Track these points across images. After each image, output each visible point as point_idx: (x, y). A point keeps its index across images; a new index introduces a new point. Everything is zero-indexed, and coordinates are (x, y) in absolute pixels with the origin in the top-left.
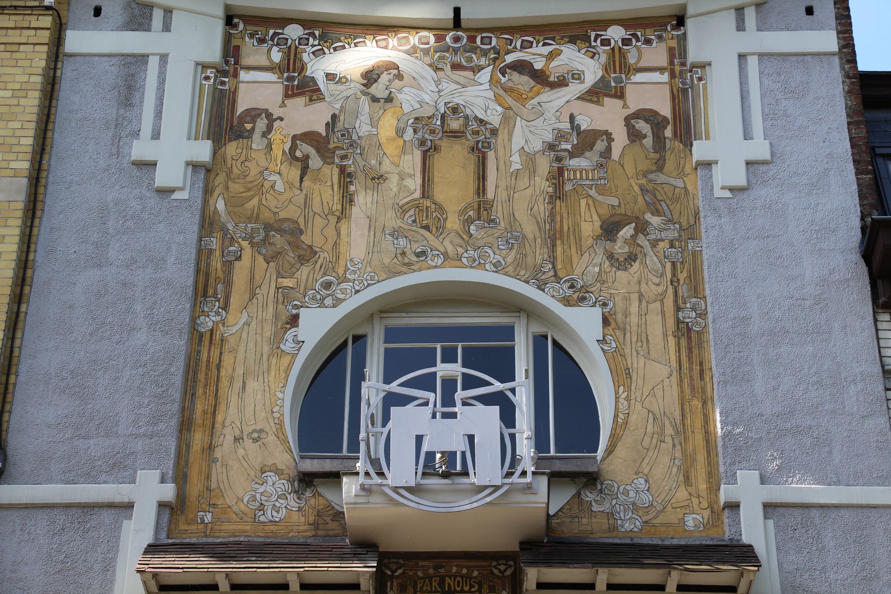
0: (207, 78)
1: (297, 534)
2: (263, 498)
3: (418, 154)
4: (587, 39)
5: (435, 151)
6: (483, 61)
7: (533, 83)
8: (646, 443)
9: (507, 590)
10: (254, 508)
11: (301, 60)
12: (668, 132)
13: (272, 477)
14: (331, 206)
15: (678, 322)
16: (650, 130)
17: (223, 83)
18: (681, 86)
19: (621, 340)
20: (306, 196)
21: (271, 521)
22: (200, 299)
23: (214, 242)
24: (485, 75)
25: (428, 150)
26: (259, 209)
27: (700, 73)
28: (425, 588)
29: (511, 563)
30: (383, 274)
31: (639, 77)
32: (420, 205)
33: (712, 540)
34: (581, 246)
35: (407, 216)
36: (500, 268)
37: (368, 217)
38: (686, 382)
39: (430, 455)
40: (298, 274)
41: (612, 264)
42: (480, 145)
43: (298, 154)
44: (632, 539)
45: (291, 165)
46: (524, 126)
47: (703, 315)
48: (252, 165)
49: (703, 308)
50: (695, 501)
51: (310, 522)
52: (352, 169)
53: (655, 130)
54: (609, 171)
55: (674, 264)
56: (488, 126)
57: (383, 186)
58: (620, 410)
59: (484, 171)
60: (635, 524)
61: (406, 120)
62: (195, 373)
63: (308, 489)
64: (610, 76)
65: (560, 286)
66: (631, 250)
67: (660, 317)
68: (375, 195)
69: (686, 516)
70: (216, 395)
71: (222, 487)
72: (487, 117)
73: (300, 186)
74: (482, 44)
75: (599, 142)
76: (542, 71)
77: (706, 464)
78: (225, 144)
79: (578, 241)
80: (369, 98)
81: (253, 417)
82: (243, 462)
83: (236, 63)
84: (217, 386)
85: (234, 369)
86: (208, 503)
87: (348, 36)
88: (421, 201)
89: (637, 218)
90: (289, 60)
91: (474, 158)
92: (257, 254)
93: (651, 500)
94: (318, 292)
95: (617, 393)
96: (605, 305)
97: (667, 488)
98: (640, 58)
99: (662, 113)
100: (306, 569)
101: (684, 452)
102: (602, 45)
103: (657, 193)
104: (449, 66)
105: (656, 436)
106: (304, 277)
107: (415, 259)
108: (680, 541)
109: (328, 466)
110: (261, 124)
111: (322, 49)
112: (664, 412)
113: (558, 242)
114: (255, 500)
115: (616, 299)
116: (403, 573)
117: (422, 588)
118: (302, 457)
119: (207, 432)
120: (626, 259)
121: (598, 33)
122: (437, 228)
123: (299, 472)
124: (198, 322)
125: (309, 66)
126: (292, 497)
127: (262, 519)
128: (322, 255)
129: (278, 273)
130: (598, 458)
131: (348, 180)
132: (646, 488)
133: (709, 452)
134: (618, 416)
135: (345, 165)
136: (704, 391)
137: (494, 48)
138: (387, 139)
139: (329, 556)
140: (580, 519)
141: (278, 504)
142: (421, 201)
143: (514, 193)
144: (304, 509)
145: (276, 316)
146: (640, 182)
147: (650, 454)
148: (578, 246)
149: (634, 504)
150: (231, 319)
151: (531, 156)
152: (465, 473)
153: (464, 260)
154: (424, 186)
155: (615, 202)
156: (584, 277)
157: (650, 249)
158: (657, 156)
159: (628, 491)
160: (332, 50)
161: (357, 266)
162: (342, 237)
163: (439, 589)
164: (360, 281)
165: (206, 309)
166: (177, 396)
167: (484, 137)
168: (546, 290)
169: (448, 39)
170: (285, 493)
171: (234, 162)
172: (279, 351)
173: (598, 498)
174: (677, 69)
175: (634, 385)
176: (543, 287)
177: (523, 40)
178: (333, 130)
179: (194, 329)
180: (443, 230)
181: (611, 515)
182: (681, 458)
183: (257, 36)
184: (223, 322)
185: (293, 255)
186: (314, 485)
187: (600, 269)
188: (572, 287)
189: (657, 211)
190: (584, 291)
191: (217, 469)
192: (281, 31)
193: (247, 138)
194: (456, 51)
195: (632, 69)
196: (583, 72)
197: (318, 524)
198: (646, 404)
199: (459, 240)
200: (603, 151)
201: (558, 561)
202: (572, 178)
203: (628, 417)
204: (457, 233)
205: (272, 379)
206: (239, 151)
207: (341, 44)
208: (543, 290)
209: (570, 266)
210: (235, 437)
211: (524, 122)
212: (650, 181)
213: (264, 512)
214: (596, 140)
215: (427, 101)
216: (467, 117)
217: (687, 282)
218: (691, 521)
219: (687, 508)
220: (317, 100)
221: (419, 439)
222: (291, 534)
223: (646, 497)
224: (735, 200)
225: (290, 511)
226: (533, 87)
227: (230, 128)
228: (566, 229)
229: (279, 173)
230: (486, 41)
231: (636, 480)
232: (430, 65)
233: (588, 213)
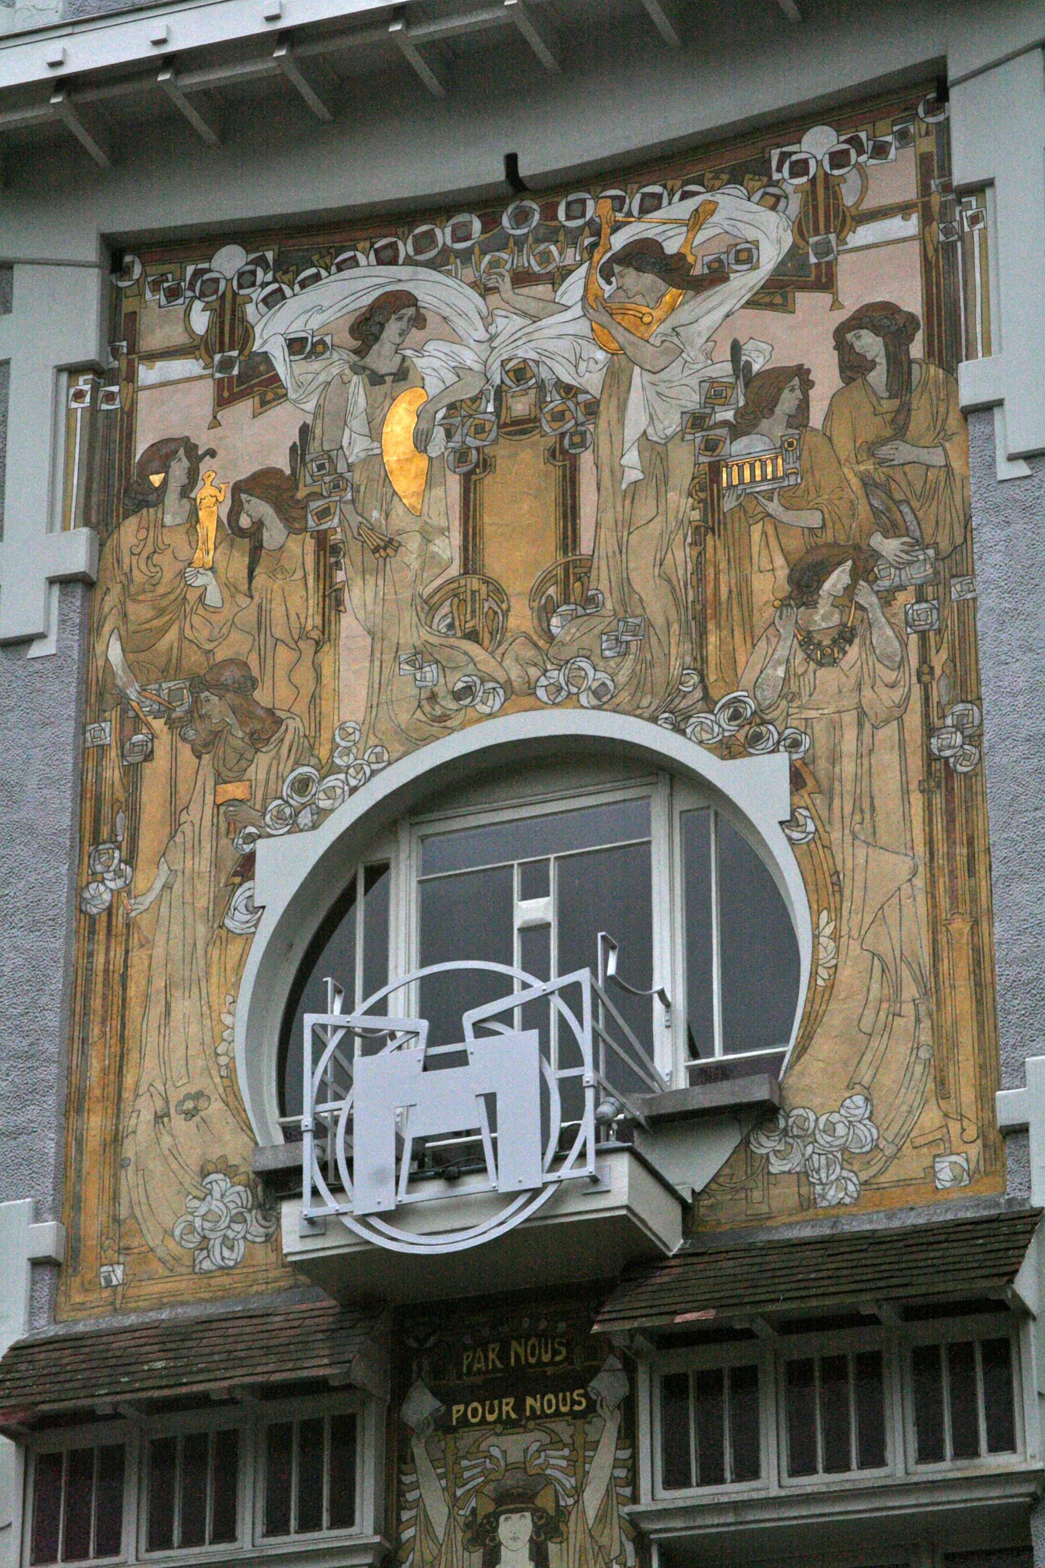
0: (79, 395)
3: (454, 483)
4: (762, 169)
5: (484, 471)
6: (571, 256)
7: (661, 285)
8: (866, 1025)
10: (192, 1246)
11: (243, 319)
12: (917, 349)
13: (219, 1183)
14: (303, 621)
15: (930, 758)
16: (883, 352)
17: (110, 397)
18: (942, 238)
19: (825, 814)
20: (260, 607)
21: (221, 1268)
22: (88, 848)
23: (107, 730)
24: (573, 289)
25: (472, 472)
26: (180, 648)
27: (974, 203)
28: (476, 1366)
30: (397, 746)
31: (864, 235)
32: (462, 590)
34: (752, 627)
35: (436, 620)
36: (605, 699)
37: (369, 632)
38: (942, 883)
40: (251, 772)
41: (809, 656)
42: (566, 442)
43: (245, 522)
45: (232, 546)
46: (647, 384)
47: (975, 738)
48: (164, 560)
49: (976, 722)
50: (954, 1127)
52: (339, 536)
53: (891, 349)
54: (805, 453)
55: (923, 636)
56: (581, 398)
57: (394, 562)
59: (574, 497)
61: (432, 411)
62: (86, 997)
64: (807, 243)
65: (712, 717)
66: (845, 619)
67: (896, 752)
68: (380, 582)
70: (122, 1038)
71: (138, 1214)
72: (579, 380)
73: (249, 588)
74: (569, 217)
75: (786, 394)
76: (680, 256)
78: (118, 526)
79: (747, 618)
80: (367, 381)
82: (171, 1159)
83: (132, 349)
84: (123, 1017)
85: (149, 982)
87: (324, 252)
88: (463, 582)
89: (857, 548)
90: (222, 323)
91: (555, 472)
92: (180, 744)
93: (875, 1137)
94: (287, 802)
95: (815, 925)
96: (796, 744)
97: (905, 1108)
98: (864, 190)
99: (905, 309)
101: (936, 1030)
102: (793, 174)
103: (894, 486)
104: (508, 279)
105: (885, 1006)
106: (262, 776)
107: (453, 705)
110: (179, 469)
111: (280, 289)
113: (711, 626)
115: (817, 729)
116: (435, 1345)
117: (470, 1367)
119: (109, 1110)
120: (834, 642)
121: (785, 149)
122: (491, 634)
124: (86, 895)
125: (258, 330)
127: (206, 1265)
128: (292, 724)
129: (218, 774)
131: (333, 560)
132: (867, 1115)
133: (981, 1025)
135: (326, 531)
136: (974, 900)
137: (590, 223)
138: (399, 461)
141: (230, 1234)
142: (463, 582)
143: (629, 534)
145: (217, 863)
146: (862, 468)
147: (874, 1043)
148: (748, 627)
149: (844, 1149)
150: (141, 884)
151: (660, 449)
153: (541, 693)
154: (465, 549)
155: (814, 519)
156: (758, 694)
157: (879, 614)
158: (897, 402)
159: (834, 1124)
160: (297, 287)
161: (352, 737)
162: (325, 681)
163: (499, 1365)
164: (358, 768)
165: (99, 868)
166: (51, 1048)
167: (573, 422)
168: (689, 730)
169: (505, 221)
171: (134, 559)
172: (224, 933)
173: (781, 1147)
174: (936, 200)
175: (846, 905)
176: (683, 726)
177: (644, 195)
178: (303, 459)
179: (81, 911)
180: (503, 635)
181: (803, 1176)
183: (166, 285)
184: (128, 889)
185: (240, 734)
187: (787, 671)
188: (735, 716)
189: (894, 525)
190: (758, 721)
191: (129, 1177)
192: (206, 265)
193: (155, 505)
194: (519, 243)
195: (849, 219)
196: (756, 243)
198: (870, 938)
199: (530, 653)
200: (794, 412)
202: (735, 482)
204: (528, 637)
205: (213, 989)
206: (143, 534)
207: (313, 271)
208: (683, 733)
209: (731, 673)
211: (647, 376)
212: (881, 462)
214: (780, 390)
215: (469, 363)
216: (541, 386)
217: (948, 671)
218: (947, 1170)
220: (274, 400)
222: (255, 1288)
224: (1036, 480)
226: (663, 295)
227: (126, 490)
228: (724, 597)
229: (211, 569)
230: (576, 210)
232: (473, 285)
233: (765, 553)
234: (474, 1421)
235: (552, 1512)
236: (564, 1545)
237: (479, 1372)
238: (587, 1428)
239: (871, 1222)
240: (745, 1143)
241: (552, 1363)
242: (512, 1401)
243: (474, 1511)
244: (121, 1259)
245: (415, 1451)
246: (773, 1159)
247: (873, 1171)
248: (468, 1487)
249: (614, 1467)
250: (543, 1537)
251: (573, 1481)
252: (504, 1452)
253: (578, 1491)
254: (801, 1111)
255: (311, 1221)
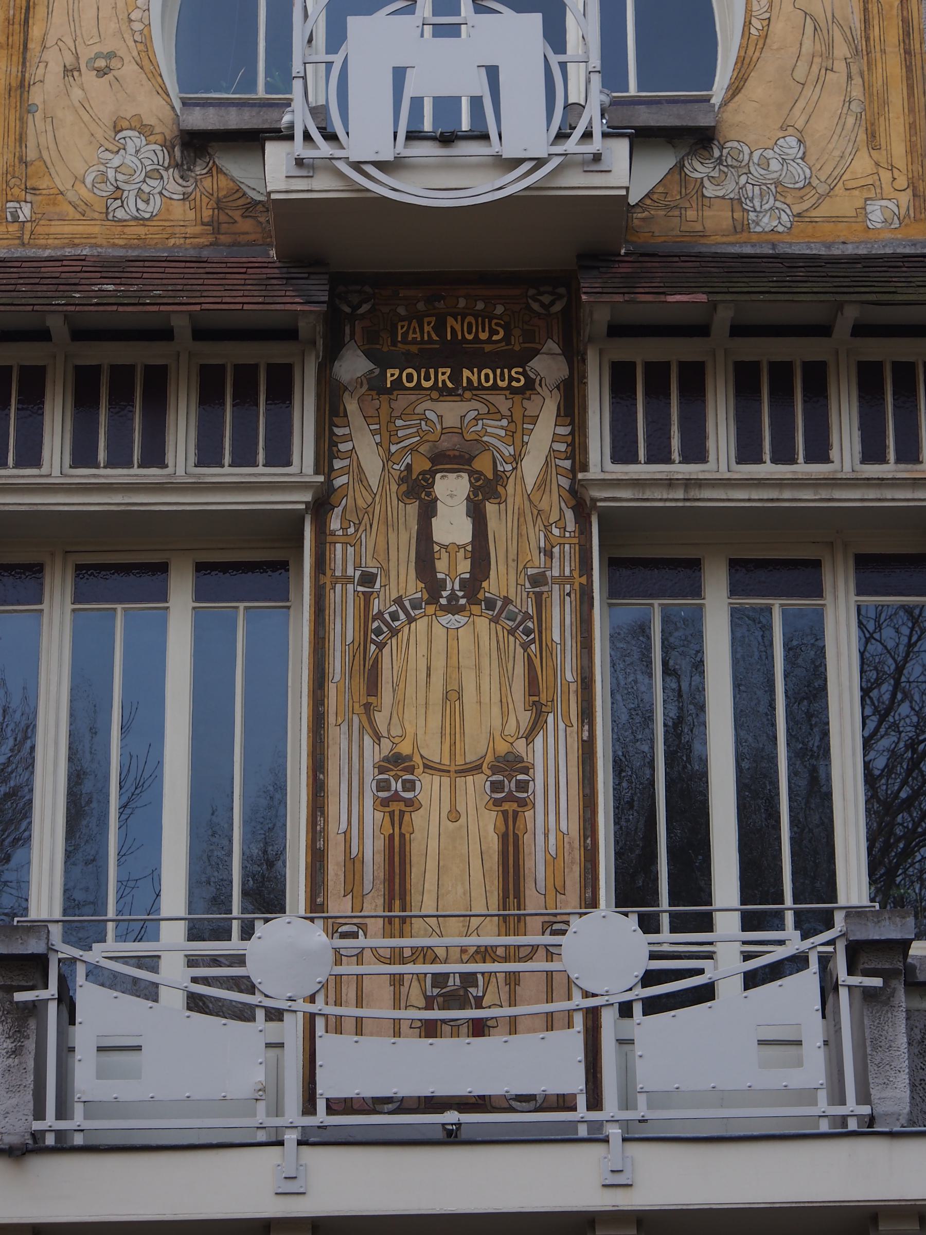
1: (182, 241)
2: (120, 177)
8: (800, 75)
9: (555, 338)
10: (104, 194)
13: (133, 140)
21: (136, 219)
28: (411, 336)
29: (562, 290)
33: (914, 245)
39: (417, 103)
44: (774, 246)
50: (886, 176)
51: (206, 220)
58: (754, 14)
60: (779, 218)
63: (199, 161)
69: (868, 202)
77: (906, 110)
81: (95, 30)
82: (82, 112)
86: (23, 187)
93: (808, 176)
97: (837, 153)
100: (205, 306)
101: (867, 88)
105: (817, 60)
108: (857, 247)
109: (234, 120)
112: (833, 16)
114: (105, 181)
116: (369, 311)
117: (405, 334)
118: (185, 103)
119: (15, 58)
123: (181, 131)
126: (170, 176)
127: (120, 214)
130: (712, 101)
132: (800, 155)
133: (910, 88)
134: (750, 23)
139: (242, 282)
140: (683, 212)
141: (146, 188)
144: (192, 197)
147: (807, 92)
149: (778, 183)
152: (485, 137)
163: (435, 338)
170: (158, 167)
173: (715, 174)
182: (862, 99)
186: (209, 154)
191: (36, 124)
197: (219, 223)
201: (647, 290)
203: (768, 25)
210: (65, 66)
213: (122, 202)
218: (878, 213)
219: (873, 191)
221: (399, 74)
222: (172, 241)
223: (801, 173)
225: (169, 201)
231: (782, 140)
234: (408, 385)
235: (490, 476)
236: (503, 506)
237: (414, 342)
238: (525, 402)
239: (811, 249)
240: (680, 166)
241: (489, 341)
242: (448, 371)
243: (409, 467)
244: (29, 198)
245: (349, 408)
246: (706, 183)
247: (805, 206)
248: (402, 444)
249: (553, 441)
250: (480, 497)
251: (511, 449)
252: (440, 417)
253: (517, 459)
254: (735, 144)
255: (299, 162)
